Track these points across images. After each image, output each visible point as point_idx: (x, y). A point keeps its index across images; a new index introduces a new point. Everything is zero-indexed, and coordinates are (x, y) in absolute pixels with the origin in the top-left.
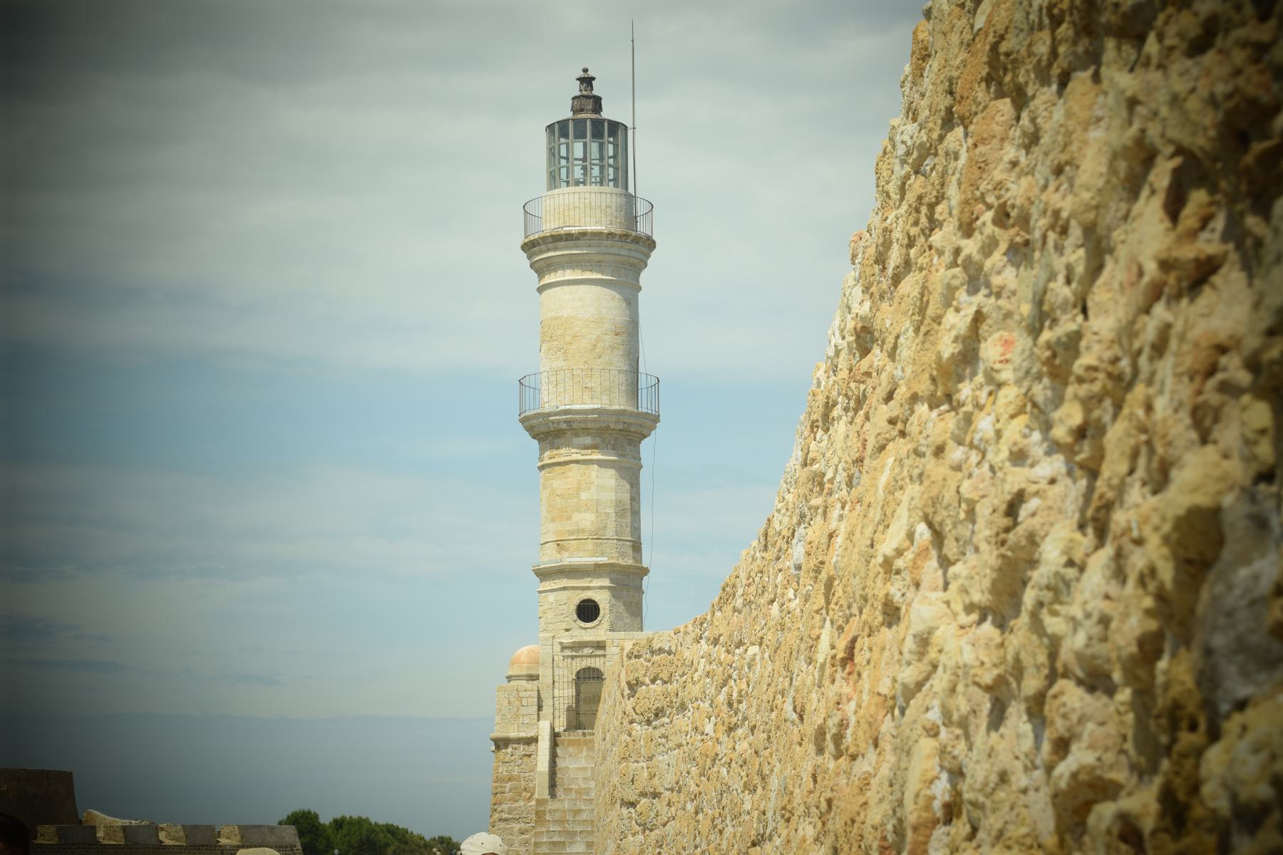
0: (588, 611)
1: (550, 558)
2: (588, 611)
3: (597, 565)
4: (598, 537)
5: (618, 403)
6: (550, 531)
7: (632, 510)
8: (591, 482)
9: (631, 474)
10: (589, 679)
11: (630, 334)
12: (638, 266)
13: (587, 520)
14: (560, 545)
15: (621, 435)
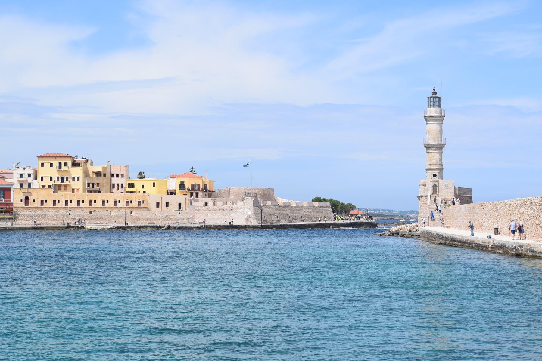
0: (435, 176)
1: (428, 167)
2: (435, 176)
3: (436, 169)
4: (436, 164)
5: (440, 143)
6: (428, 163)
7: (441, 159)
8: (435, 155)
9: (441, 155)
10: (435, 187)
11: (441, 131)
12: (442, 120)
13: (435, 161)
14: (430, 165)
15: (440, 147)
